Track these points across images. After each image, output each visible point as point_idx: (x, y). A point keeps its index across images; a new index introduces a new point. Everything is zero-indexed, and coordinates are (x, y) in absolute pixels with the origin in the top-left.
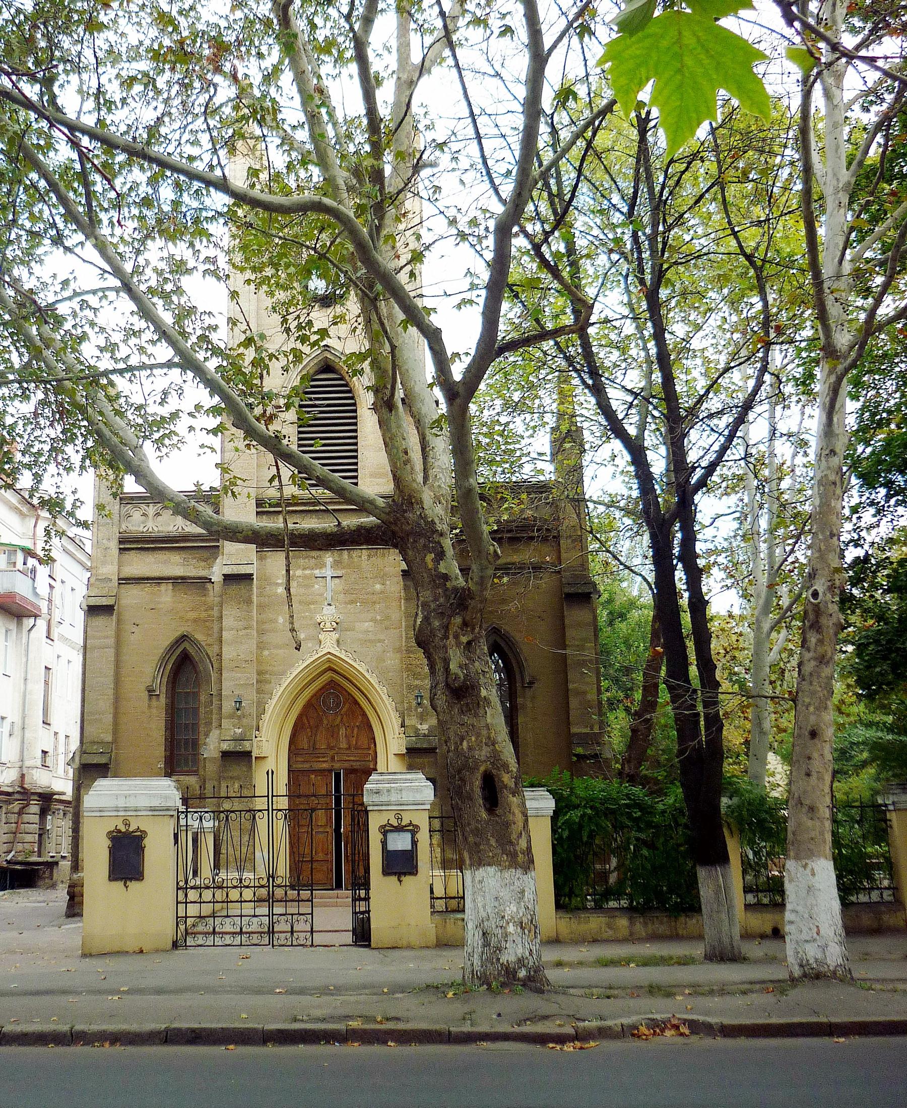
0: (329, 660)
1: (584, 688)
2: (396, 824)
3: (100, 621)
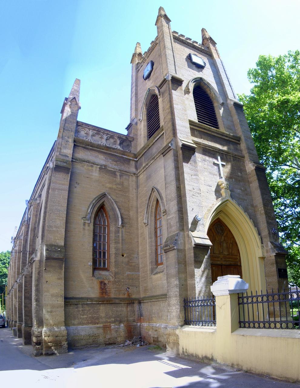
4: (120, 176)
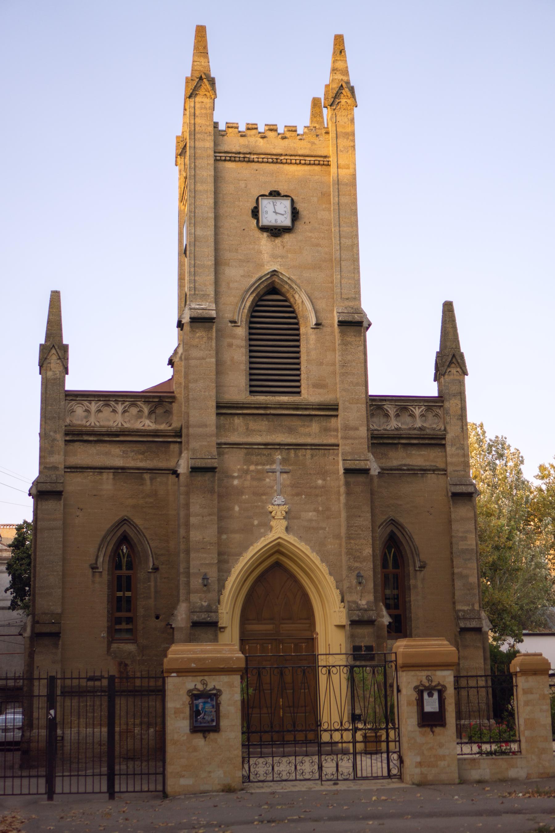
0: (279, 544)
1: (465, 572)
2: (427, 685)
3: (50, 505)
4: (151, 479)
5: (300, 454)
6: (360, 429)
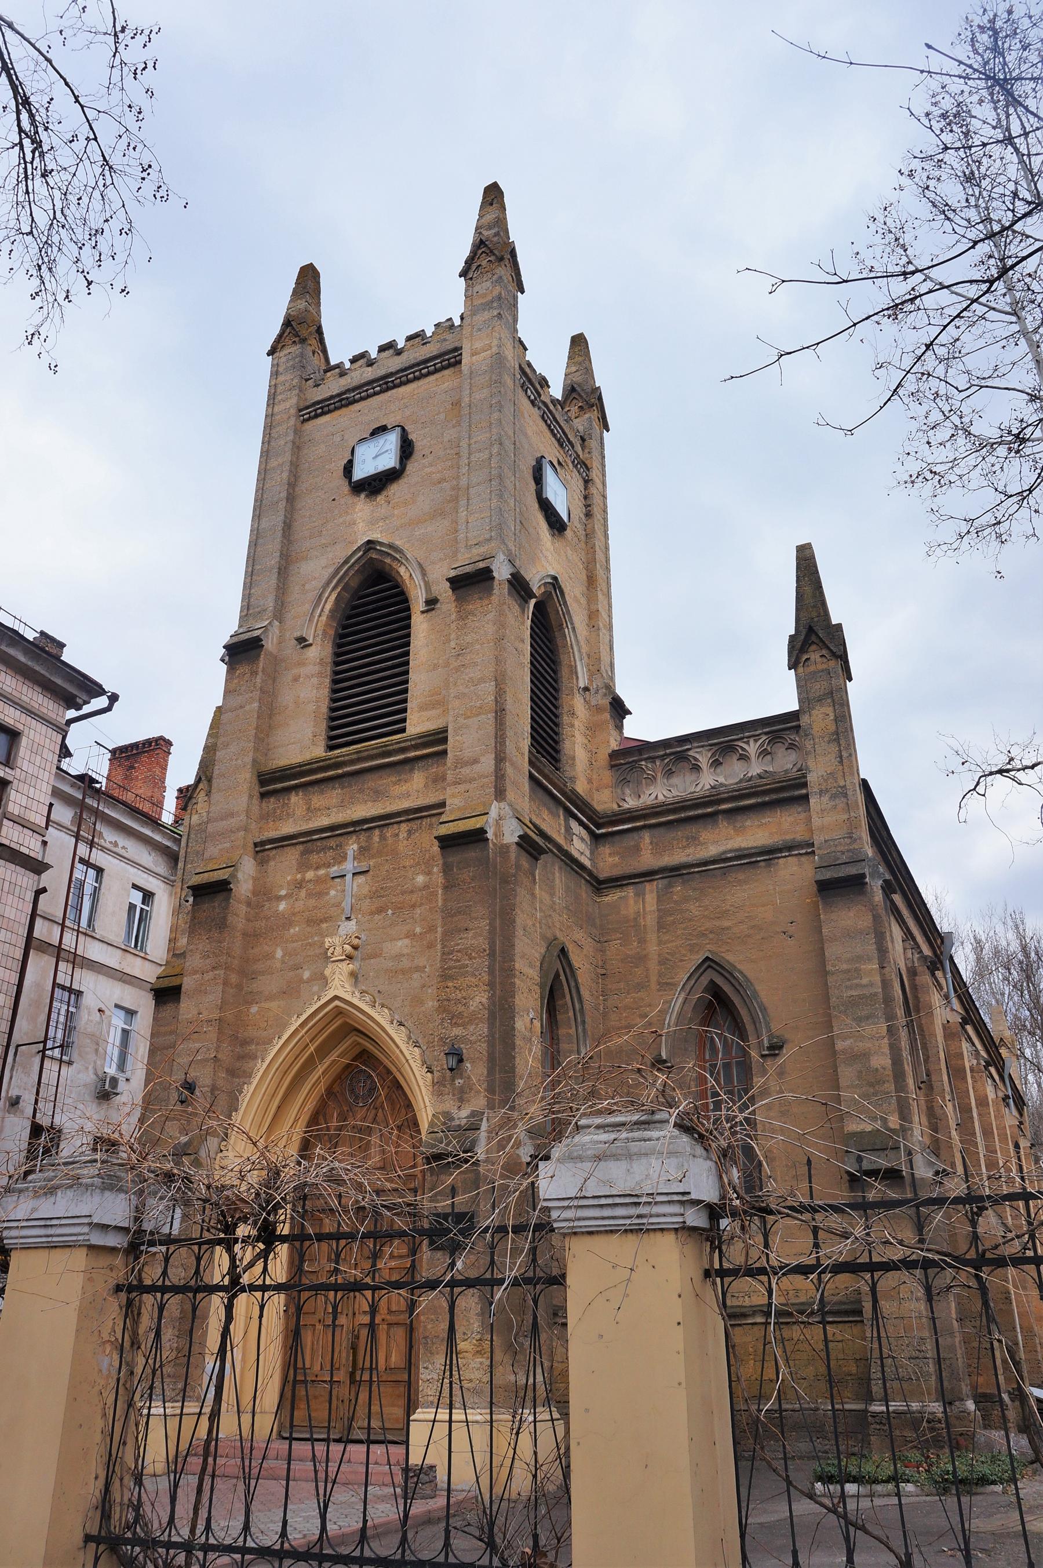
0: (339, 1012)
1: (862, 1046)
5: (388, 835)
6: (483, 759)
